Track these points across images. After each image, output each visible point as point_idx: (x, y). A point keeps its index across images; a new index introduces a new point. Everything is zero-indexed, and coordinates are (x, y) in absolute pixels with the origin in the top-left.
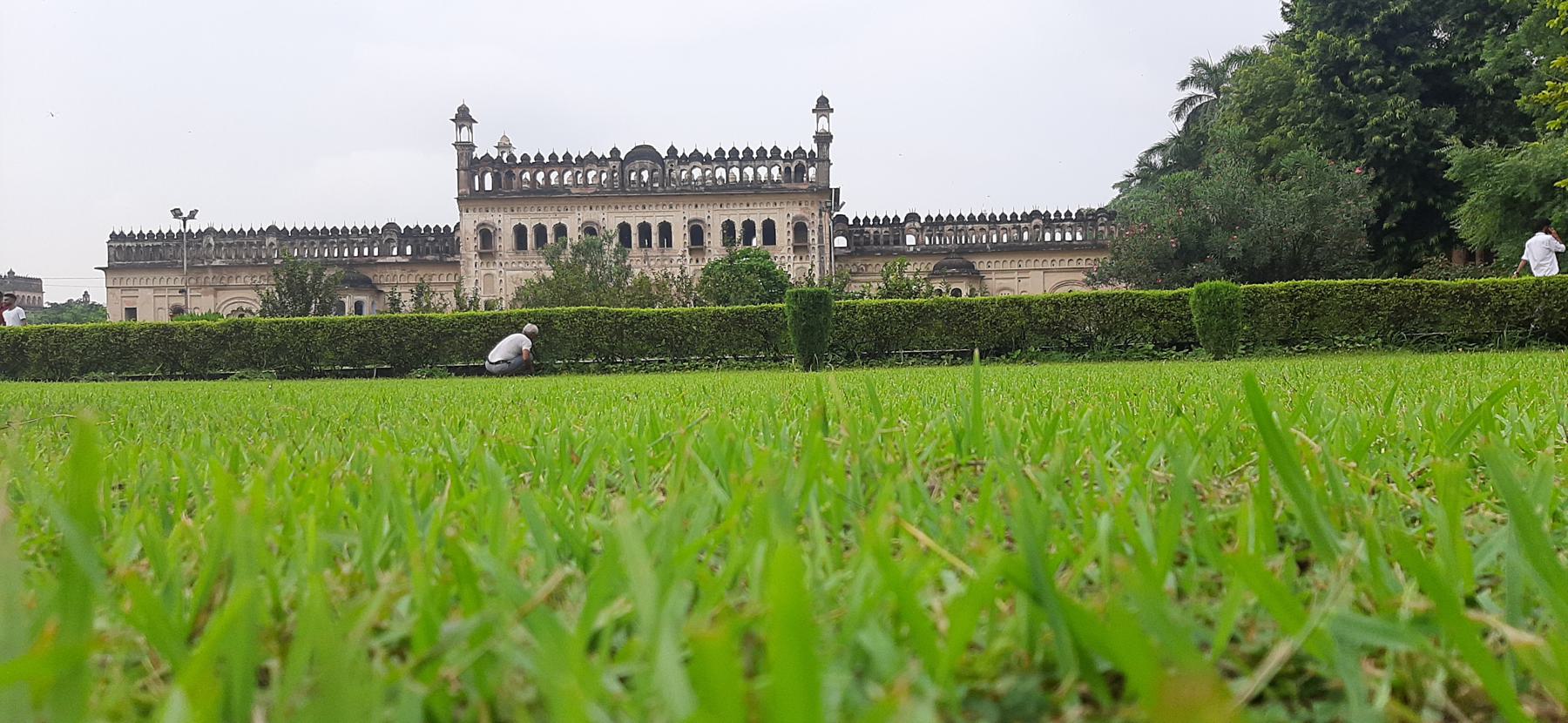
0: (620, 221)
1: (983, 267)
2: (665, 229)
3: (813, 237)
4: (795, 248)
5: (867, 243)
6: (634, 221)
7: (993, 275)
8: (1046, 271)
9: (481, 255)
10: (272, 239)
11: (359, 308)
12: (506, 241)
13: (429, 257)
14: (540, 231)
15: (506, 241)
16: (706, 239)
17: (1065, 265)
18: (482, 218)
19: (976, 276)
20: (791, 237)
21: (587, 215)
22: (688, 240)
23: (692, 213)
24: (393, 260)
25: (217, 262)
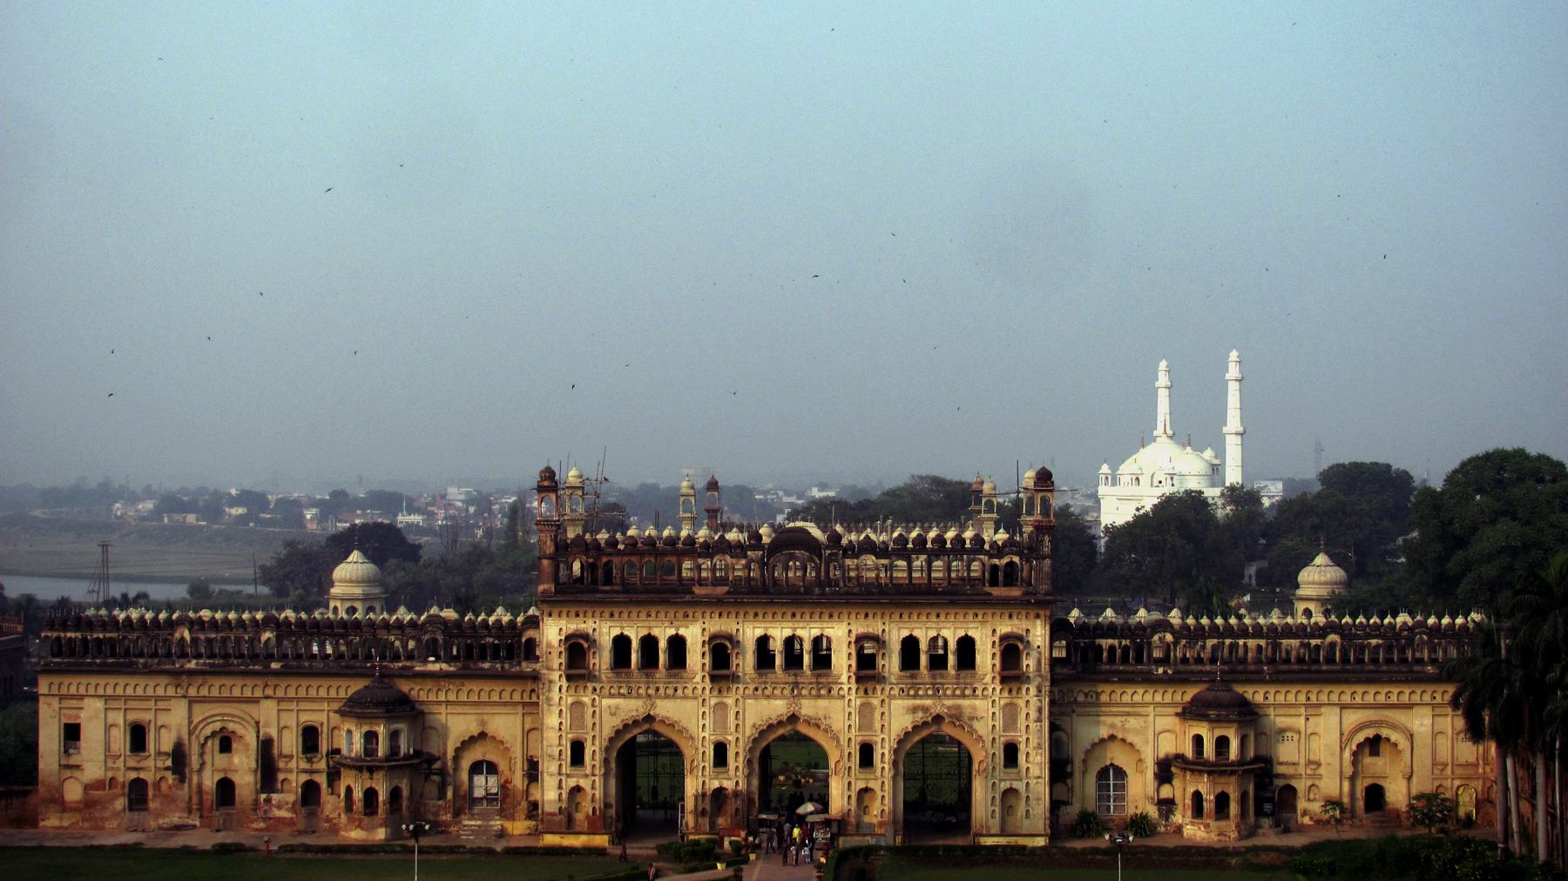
0: (759, 632)
1: (1259, 698)
3: (1029, 663)
4: (1004, 680)
6: (779, 633)
9: (569, 678)
10: (267, 635)
11: (394, 736)
12: (602, 660)
13: (487, 665)
14: (649, 643)
15: (602, 660)
17: (1369, 699)
18: (572, 626)
19: (1248, 715)
20: (997, 661)
23: (860, 627)
24: (434, 666)
25: (192, 665)
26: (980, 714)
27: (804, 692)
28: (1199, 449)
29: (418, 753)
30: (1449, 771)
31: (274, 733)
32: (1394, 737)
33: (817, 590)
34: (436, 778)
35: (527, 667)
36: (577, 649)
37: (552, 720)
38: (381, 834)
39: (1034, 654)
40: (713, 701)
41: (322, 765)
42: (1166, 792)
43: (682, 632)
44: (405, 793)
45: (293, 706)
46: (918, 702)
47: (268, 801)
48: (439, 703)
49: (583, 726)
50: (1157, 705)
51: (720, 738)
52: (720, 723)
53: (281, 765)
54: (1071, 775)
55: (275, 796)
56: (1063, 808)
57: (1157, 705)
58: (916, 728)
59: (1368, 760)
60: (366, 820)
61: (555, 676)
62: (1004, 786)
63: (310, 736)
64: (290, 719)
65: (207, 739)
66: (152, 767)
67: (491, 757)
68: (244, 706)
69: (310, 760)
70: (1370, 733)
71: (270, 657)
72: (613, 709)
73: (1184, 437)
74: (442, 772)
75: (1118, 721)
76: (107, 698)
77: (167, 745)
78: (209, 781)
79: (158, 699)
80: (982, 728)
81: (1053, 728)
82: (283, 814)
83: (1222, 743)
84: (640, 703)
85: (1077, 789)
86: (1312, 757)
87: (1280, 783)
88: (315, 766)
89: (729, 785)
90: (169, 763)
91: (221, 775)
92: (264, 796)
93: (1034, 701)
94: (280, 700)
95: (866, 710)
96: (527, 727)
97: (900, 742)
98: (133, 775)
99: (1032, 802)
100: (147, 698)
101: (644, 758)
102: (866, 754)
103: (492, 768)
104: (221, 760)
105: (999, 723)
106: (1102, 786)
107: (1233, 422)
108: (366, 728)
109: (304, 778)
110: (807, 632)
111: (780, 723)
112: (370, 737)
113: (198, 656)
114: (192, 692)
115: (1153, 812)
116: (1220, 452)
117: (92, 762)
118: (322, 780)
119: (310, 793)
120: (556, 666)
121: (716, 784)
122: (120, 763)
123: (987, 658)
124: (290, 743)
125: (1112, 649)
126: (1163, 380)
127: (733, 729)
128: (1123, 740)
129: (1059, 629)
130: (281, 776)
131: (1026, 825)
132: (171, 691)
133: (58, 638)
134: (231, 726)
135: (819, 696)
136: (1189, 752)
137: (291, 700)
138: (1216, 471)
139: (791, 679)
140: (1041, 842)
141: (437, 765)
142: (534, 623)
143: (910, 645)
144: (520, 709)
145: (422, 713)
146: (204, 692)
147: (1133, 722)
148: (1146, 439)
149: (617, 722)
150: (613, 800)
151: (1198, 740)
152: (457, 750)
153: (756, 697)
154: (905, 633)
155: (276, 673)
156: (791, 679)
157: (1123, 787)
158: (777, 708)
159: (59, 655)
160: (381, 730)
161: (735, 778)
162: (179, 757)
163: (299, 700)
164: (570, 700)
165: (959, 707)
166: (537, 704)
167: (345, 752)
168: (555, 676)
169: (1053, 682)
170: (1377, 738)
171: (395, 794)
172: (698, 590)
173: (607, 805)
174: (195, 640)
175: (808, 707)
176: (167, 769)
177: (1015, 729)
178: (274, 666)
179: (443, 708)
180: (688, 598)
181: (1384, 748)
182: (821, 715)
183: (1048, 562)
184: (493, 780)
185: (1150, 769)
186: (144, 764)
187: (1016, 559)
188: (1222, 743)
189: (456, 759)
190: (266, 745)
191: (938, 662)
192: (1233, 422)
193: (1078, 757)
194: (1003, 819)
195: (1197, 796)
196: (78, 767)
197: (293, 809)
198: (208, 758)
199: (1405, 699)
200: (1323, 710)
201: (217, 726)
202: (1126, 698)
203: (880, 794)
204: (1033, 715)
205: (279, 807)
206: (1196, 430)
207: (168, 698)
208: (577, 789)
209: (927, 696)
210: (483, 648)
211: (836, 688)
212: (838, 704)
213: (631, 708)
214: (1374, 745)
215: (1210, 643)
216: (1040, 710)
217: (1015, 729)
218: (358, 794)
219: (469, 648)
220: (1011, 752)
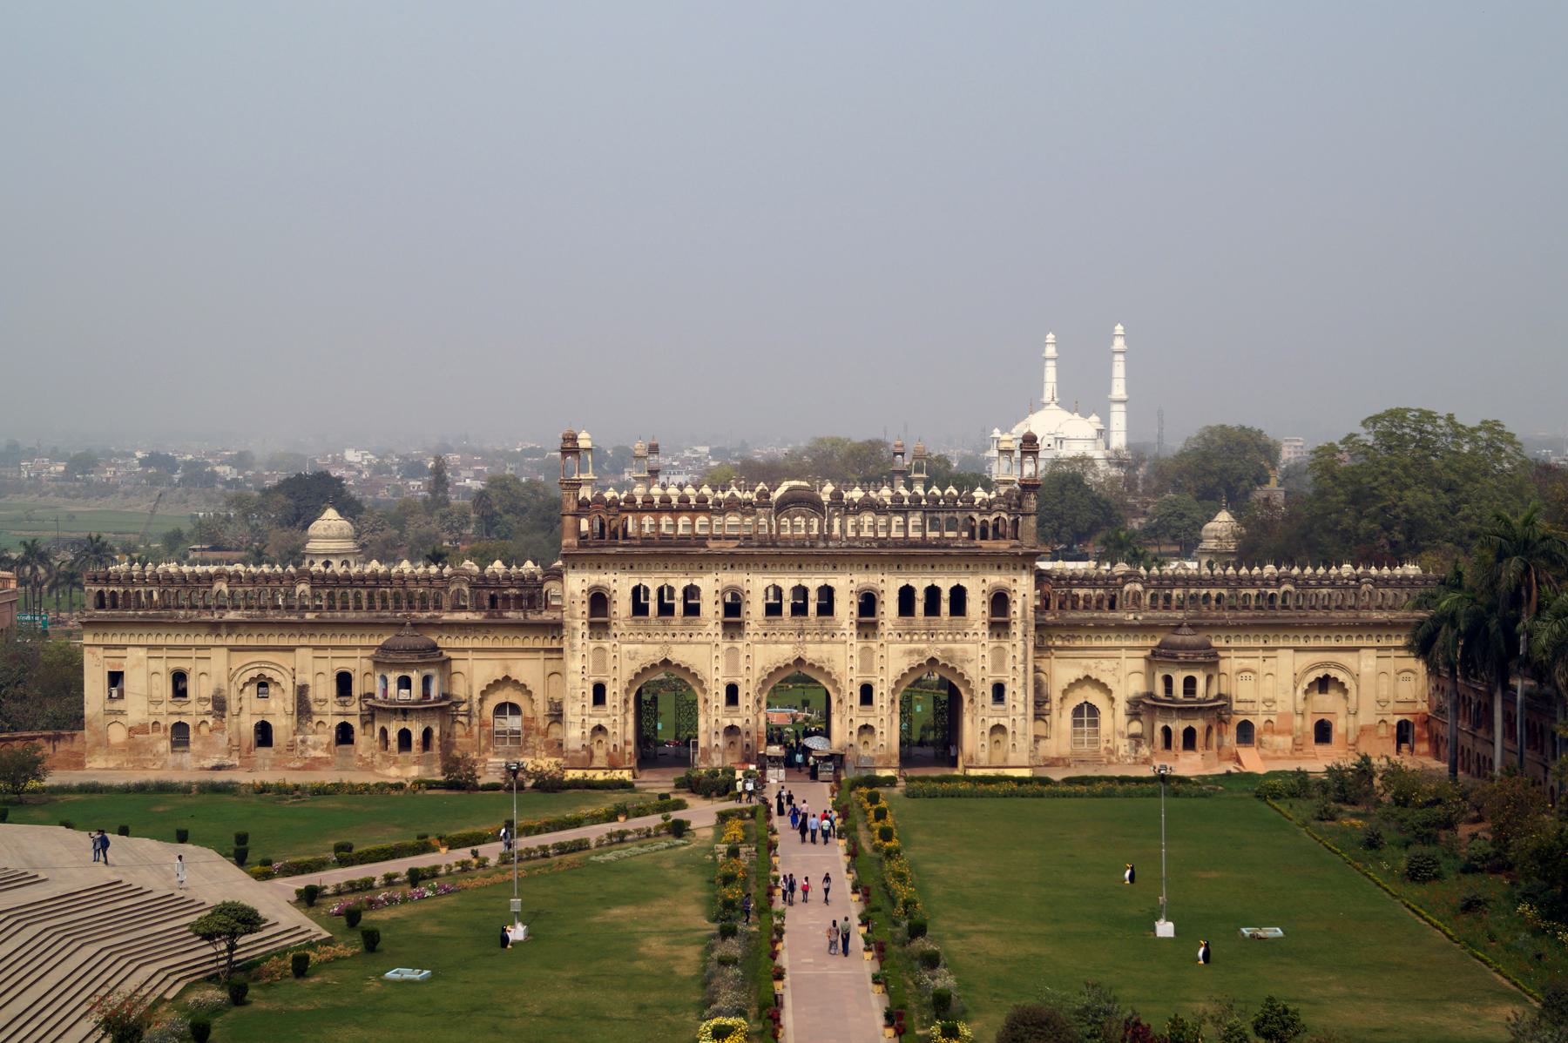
2: (827, 593)
3: (1016, 609)
4: (993, 626)
5: (1074, 607)
6: (787, 582)
7: (1233, 653)
8: (1297, 650)
9: (592, 625)
10: (303, 588)
11: (426, 681)
12: (622, 606)
13: (510, 614)
15: (622, 606)
16: (879, 608)
17: (1323, 643)
20: (986, 608)
21: (730, 578)
22: (855, 609)
25: (231, 615)
26: (970, 656)
27: (808, 638)
28: (1085, 415)
29: (445, 697)
30: (1390, 707)
31: (305, 678)
32: (1342, 677)
33: (822, 544)
34: (464, 719)
35: (547, 616)
36: (599, 601)
37: (574, 664)
38: (414, 772)
39: (1019, 602)
40: (726, 646)
41: (355, 708)
42: (1136, 727)
43: (696, 582)
44: (436, 732)
45: (329, 653)
46: (913, 646)
47: (303, 742)
48: (465, 650)
49: (604, 671)
50: (1128, 648)
51: (732, 680)
52: (733, 666)
53: (315, 708)
54: (1049, 713)
55: (311, 739)
56: (1042, 743)
57: (1128, 648)
58: (911, 669)
59: (1317, 697)
60: (401, 756)
61: (578, 624)
62: (994, 721)
63: (344, 683)
64: (322, 665)
65: (245, 684)
66: (194, 711)
67: (512, 699)
68: (280, 654)
69: (343, 704)
70: (1320, 673)
71: (305, 608)
72: (630, 652)
73: (1072, 402)
74: (469, 714)
75: (1092, 662)
76: (150, 647)
77: (209, 693)
78: (248, 724)
79: (199, 648)
80: (971, 671)
81: (1037, 670)
82: (319, 754)
83: (1190, 683)
84: (657, 647)
85: (1055, 724)
86: (1269, 695)
87: (1242, 718)
88: (349, 710)
89: (738, 722)
90: (209, 707)
91: (260, 719)
92: (299, 737)
93: (1020, 645)
94: (316, 648)
95: (866, 653)
96: (549, 671)
97: (897, 683)
98: (176, 719)
99: (1018, 737)
100: (188, 647)
101: (662, 701)
102: (867, 694)
103: (515, 709)
104: (259, 705)
105: (988, 665)
106: (1076, 723)
107: (1119, 390)
108: (398, 674)
109: (340, 720)
110: (813, 582)
111: (787, 665)
112: (405, 683)
113: (237, 608)
114: (231, 641)
115: (1124, 746)
116: (1106, 420)
117: (136, 708)
118: (355, 722)
119: (345, 734)
120: (579, 614)
121: (728, 722)
122: (162, 708)
123: (977, 606)
124: (324, 688)
125: (1087, 599)
126: (1050, 351)
127: (743, 670)
128: (1097, 681)
129: (1041, 577)
130: (316, 719)
131: (1013, 759)
132: (210, 641)
133: (101, 593)
134: (268, 673)
135: (822, 642)
136: (1160, 691)
137: (324, 648)
138: (1103, 433)
139: (797, 625)
140: (1026, 773)
141: (464, 707)
142: (558, 575)
143: (906, 595)
144: (542, 655)
145: (450, 659)
146: (243, 641)
147: (1106, 664)
148: (1036, 405)
149: (636, 666)
150: (631, 736)
151: (1168, 681)
152: (483, 693)
153: (765, 643)
154: (903, 583)
155: (311, 624)
156: (797, 625)
157: (1095, 723)
158: (782, 652)
159: (101, 606)
160: (416, 677)
161: (749, 715)
162: (219, 705)
163: (334, 648)
164: (592, 646)
165: (951, 650)
166: (560, 650)
167: (379, 695)
168: (578, 624)
169: (1037, 627)
170: (1327, 677)
171: (427, 734)
172: (712, 545)
173: (626, 743)
174: (232, 594)
175: (813, 652)
176: (208, 713)
177: (1003, 670)
178: (309, 616)
179: (470, 655)
180: (702, 550)
181: (1331, 685)
182: (825, 656)
183: (1033, 518)
184: (513, 723)
185: (1122, 706)
186: (185, 709)
187: (1004, 515)
188: (1190, 683)
189: (481, 701)
190: (302, 691)
191: (932, 607)
192: (1119, 390)
193: (1056, 695)
194: (991, 753)
195: (1167, 732)
196: (122, 713)
197: (328, 749)
198: (245, 703)
199: (1355, 643)
200: (1280, 652)
201: (255, 673)
202: (1096, 643)
203: (878, 730)
204: (1020, 657)
205: (315, 748)
206: (1083, 396)
207: (208, 647)
208: (600, 729)
209: (920, 641)
210: (506, 598)
211: (839, 633)
212: (841, 647)
213: (650, 652)
214: (1324, 684)
215: (1176, 592)
216: (1025, 653)
217: (1003, 670)
218: (393, 735)
219: (493, 599)
220: (999, 691)
